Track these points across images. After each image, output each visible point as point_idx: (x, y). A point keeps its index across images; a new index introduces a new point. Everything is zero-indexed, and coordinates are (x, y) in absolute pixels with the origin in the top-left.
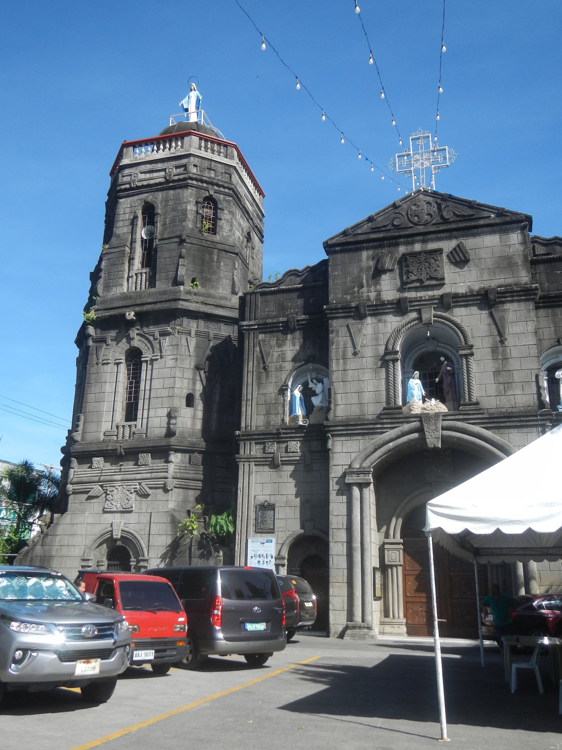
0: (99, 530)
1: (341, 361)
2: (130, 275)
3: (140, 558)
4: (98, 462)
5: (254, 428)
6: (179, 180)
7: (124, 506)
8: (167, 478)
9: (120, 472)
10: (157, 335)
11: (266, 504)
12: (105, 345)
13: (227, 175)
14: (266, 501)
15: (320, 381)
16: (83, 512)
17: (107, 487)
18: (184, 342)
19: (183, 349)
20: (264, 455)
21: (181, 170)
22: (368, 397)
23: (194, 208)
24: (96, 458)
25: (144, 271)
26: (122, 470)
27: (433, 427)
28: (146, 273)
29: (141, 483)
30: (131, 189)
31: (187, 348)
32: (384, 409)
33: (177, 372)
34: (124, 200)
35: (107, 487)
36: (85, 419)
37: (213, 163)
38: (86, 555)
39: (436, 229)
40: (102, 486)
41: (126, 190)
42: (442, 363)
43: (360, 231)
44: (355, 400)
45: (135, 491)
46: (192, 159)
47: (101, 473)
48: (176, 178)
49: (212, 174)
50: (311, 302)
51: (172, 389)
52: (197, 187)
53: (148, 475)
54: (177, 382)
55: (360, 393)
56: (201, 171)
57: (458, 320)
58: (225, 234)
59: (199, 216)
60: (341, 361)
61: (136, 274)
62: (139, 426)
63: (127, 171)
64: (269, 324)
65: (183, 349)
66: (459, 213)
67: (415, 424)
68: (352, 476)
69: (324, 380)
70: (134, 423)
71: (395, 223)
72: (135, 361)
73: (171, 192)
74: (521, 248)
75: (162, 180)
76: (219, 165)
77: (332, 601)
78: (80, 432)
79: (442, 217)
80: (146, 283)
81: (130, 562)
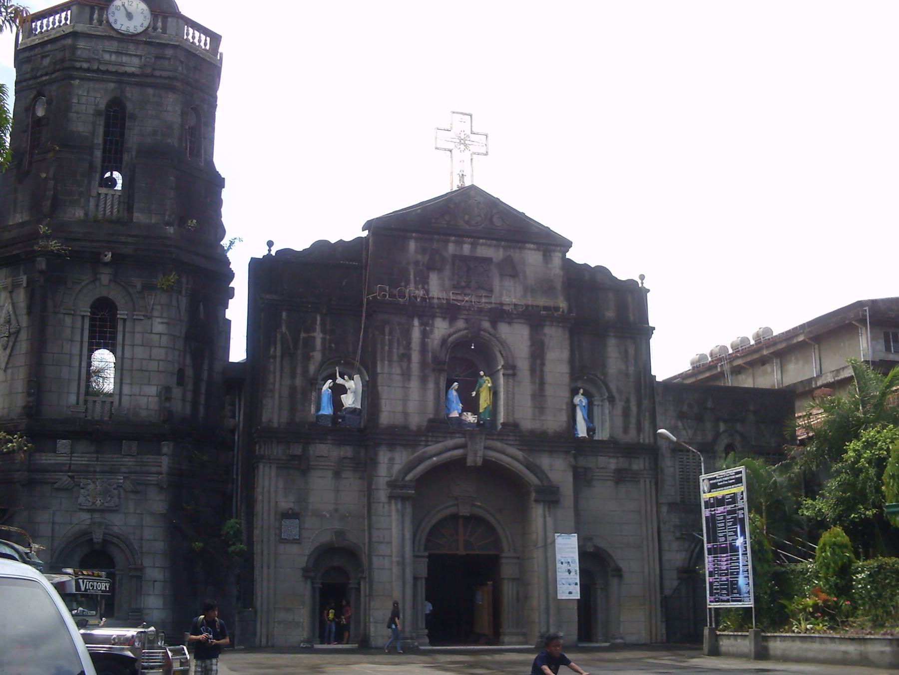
1: (386, 363)
6: (161, 77)
7: (106, 505)
9: (97, 460)
10: (139, 286)
11: (290, 511)
14: (291, 509)
15: (351, 378)
17: (80, 478)
22: (412, 407)
26: (99, 459)
30: (88, 70)
32: (430, 421)
40: (72, 477)
41: (81, 69)
44: (400, 408)
45: (118, 486)
50: (344, 283)
55: (405, 400)
60: (386, 363)
62: (116, 404)
63: (81, 44)
73: (150, 91)
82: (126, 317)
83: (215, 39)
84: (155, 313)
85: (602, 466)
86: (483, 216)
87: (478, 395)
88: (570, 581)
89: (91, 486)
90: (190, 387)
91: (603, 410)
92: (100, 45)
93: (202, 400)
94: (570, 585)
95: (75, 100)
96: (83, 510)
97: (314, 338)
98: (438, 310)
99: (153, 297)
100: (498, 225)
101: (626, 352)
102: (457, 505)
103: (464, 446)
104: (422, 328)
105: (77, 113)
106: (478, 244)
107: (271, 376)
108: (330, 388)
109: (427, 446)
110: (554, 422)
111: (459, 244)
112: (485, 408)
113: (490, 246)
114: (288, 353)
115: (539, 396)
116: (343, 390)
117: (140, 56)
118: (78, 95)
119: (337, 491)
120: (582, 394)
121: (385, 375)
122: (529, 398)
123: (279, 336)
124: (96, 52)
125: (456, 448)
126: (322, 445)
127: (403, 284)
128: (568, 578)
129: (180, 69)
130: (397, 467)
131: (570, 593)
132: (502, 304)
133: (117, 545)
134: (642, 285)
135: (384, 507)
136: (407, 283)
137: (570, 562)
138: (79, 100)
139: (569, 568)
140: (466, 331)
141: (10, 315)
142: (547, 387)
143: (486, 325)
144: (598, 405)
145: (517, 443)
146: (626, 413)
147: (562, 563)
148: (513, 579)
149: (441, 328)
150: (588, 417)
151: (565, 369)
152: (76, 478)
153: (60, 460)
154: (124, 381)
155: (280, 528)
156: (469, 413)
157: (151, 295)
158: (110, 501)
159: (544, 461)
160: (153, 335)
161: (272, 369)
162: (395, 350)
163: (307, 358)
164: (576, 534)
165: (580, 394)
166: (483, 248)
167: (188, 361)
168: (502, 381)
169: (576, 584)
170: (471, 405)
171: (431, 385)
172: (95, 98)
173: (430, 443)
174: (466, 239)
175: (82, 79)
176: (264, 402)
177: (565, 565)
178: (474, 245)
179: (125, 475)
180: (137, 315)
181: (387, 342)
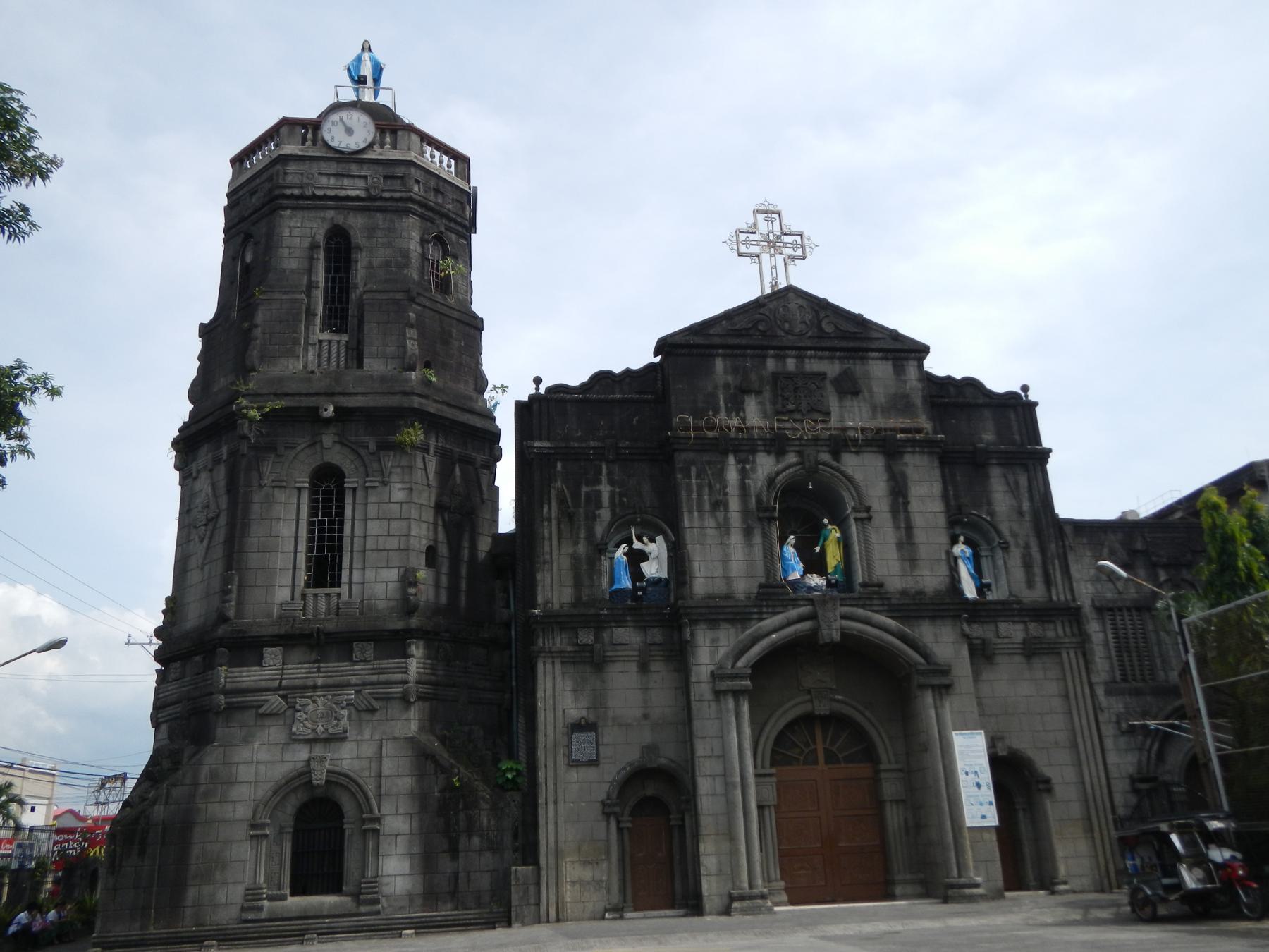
0: (280, 772)
1: (696, 514)
2: (311, 342)
3: (364, 816)
4: (272, 655)
5: (556, 607)
6: (392, 199)
7: (331, 731)
8: (407, 683)
9: (319, 671)
10: (372, 446)
11: (583, 722)
12: (273, 456)
13: (459, 205)
14: (583, 718)
15: (652, 540)
16: (246, 741)
18: (420, 464)
19: (419, 475)
20: (577, 648)
21: (397, 184)
22: (737, 568)
23: (419, 249)
24: (270, 650)
25: (335, 337)
27: (830, 615)
28: (338, 342)
29: (360, 691)
30: (302, 197)
31: (424, 472)
32: (761, 586)
33: (413, 511)
34: (288, 212)
35: (295, 698)
36: (240, 581)
37: (441, 183)
38: (258, 816)
39: (818, 345)
40: (284, 697)
41: (292, 197)
42: (826, 526)
43: (711, 332)
44: (719, 572)
46: (413, 170)
47: (282, 674)
48: (387, 195)
49: (440, 200)
50: (635, 422)
51: (403, 539)
52: (422, 217)
53: (375, 678)
54: (413, 527)
55: (725, 561)
56: (426, 192)
57: (850, 472)
58: (460, 296)
59: (426, 263)
60: (696, 514)
61: (320, 342)
62: (345, 596)
63: (292, 168)
64: (574, 448)
65: (419, 475)
66: (842, 328)
67: (804, 610)
69: (657, 538)
70: (336, 590)
71: (761, 327)
72: (326, 487)
73: (379, 216)
74: (920, 385)
75: (362, 194)
76: (449, 188)
77: (705, 862)
78: (233, 603)
79: (821, 329)
80: (338, 356)
81: (343, 824)
82: (356, 485)
83: (462, 161)
84: (394, 478)
85: (1005, 634)
86: (808, 322)
87: (823, 550)
88: (981, 799)
89: (311, 707)
90: (445, 569)
91: (994, 562)
92: (315, 168)
93: (463, 585)
94: (981, 804)
95: (286, 233)
96: (299, 741)
97: (599, 493)
98: (759, 443)
99: (391, 457)
100: (827, 331)
101: (1017, 483)
102: (811, 701)
103: (812, 617)
104: (740, 467)
105: (289, 248)
106: (805, 357)
107: (547, 543)
108: (625, 554)
109: (761, 620)
110: (931, 579)
111: (781, 358)
112: (835, 567)
113: (821, 358)
114: (568, 516)
115: (907, 544)
116: (643, 556)
117: (365, 177)
118: (290, 227)
119: (645, 690)
120: (964, 543)
121: (695, 530)
122: (894, 547)
123: (553, 493)
124: (310, 176)
125: (801, 619)
126: (619, 629)
127: (711, 413)
128: (977, 796)
129: (416, 189)
130: (722, 651)
131: (984, 817)
132: (845, 429)
133: (346, 788)
134: (1027, 396)
135: (709, 707)
136: (716, 411)
137: (979, 772)
138: (290, 232)
139: (978, 780)
140: (798, 467)
141: (209, 499)
142: (916, 532)
143: (825, 457)
144: (986, 556)
145: (886, 608)
146: (1027, 565)
147: (967, 773)
148: (897, 802)
149: (765, 465)
150: (975, 570)
151: (937, 507)
152: (291, 698)
153: (268, 673)
154: (355, 565)
155: (569, 746)
156: (815, 575)
157: (389, 456)
158: (337, 725)
159: (926, 633)
160: (392, 505)
161: (546, 535)
162: (706, 497)
163: (592, 518)
164: (982, 731)
165: (960, 543)
166: (813, 361)
167: (441, 536)
168: (854, 528)
169: (991, 803)
170: (815, 564)
171: (757, 539)
172: (312, 228)
173: (765, 616)
174: (789, 352)
175: (294, 208)
176: (539, 577)
177: (971, 776)
178: (800, 358)
179: (357, 688)
180: (371, 481)
181: (695, 488)
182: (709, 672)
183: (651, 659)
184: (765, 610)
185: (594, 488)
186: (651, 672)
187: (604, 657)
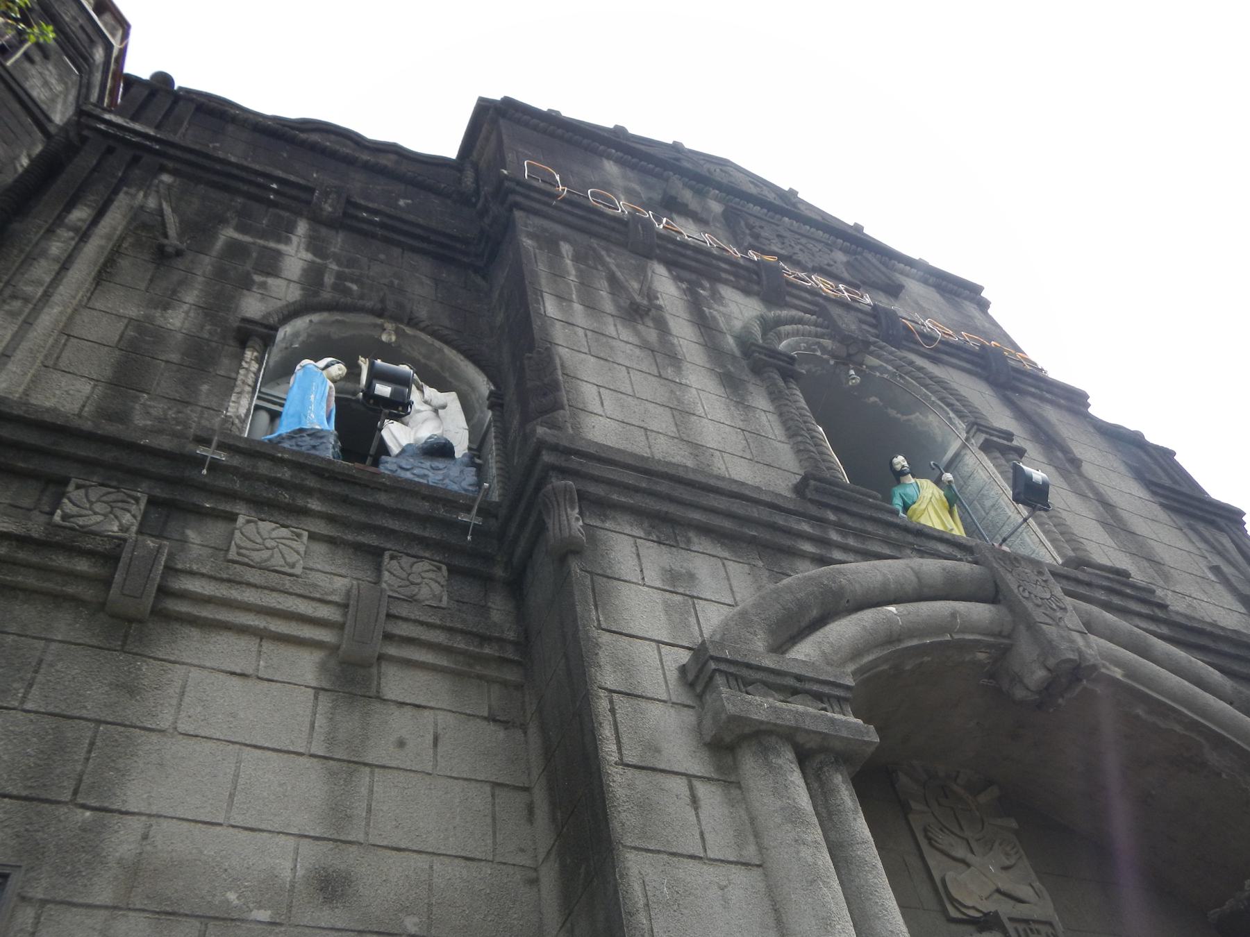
42: (899, 475)
68: (750, 688)
135: (694, 801)
182: (673, 675)
183: (392, 650)
184: (834, 536)
185: (261, 242)
186: (380, 699)
187: (164, 591)
